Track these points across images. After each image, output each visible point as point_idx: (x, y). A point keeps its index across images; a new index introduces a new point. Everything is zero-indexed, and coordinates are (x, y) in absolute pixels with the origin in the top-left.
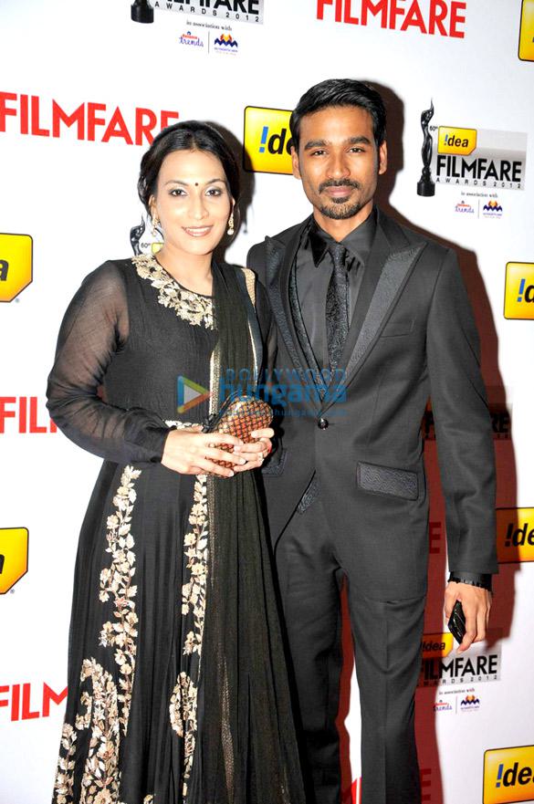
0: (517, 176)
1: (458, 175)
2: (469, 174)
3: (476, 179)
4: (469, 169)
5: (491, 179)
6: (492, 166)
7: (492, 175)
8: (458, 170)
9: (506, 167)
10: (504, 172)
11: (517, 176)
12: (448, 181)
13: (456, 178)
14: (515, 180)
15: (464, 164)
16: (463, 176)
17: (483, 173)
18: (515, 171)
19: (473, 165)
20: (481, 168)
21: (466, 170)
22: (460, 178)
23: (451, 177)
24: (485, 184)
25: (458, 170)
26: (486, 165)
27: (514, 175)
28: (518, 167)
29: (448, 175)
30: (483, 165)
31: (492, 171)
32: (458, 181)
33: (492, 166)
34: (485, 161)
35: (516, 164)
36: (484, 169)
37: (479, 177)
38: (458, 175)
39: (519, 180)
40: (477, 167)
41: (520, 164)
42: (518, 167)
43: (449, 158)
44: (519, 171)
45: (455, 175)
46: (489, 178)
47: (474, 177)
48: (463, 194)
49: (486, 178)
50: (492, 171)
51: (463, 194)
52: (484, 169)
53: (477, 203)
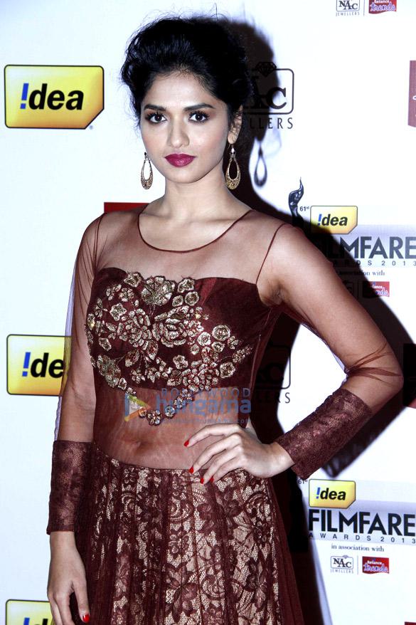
0: (410, 530)
1: (335, 530)
2: (348, 529)
3: (358, 533)
4: (348, 523)
5: (377, 534)
6: (377, 519)
7: (377, 529)
8: (335, 524)
9: (394, 520)
10: (391, 525)
11: (410, 530)
12: (323, 536)
13: (332, 533)
14: (407, 534)
15: (342, 519)
16: (341, 530)
17: (367, 527)
18: (407, 525)
19: (354, 519)
20: (363, 522)
21: (344, 524)
22: (338, 533)
23: (326, 532)
24: (369, 539)
25: (335, 524)
26: (371, 519)
27: (406, 529)
28: (410, 520)
29: (323, 529)
30: (365, 518)
31: (377, 525)
32: (335, 536)
33: (377, 519)
34: (368, 514)
35: (407, 517)
36: (368, 522)
37: (362, 531)
38: (335, 530)
39: (413, 534)
40: (357, 521)
41: (413, 516)
42: (410, 520)
43: (323, 512)
44: (413, 525)
45: (330, 529)
46: (374, 532)
47: (355, 531)
48: (333, 547)
49: (370, 532)
50: (377, 525)
51: (333, 547)
52: (368, 522)
53: (356, 558)
